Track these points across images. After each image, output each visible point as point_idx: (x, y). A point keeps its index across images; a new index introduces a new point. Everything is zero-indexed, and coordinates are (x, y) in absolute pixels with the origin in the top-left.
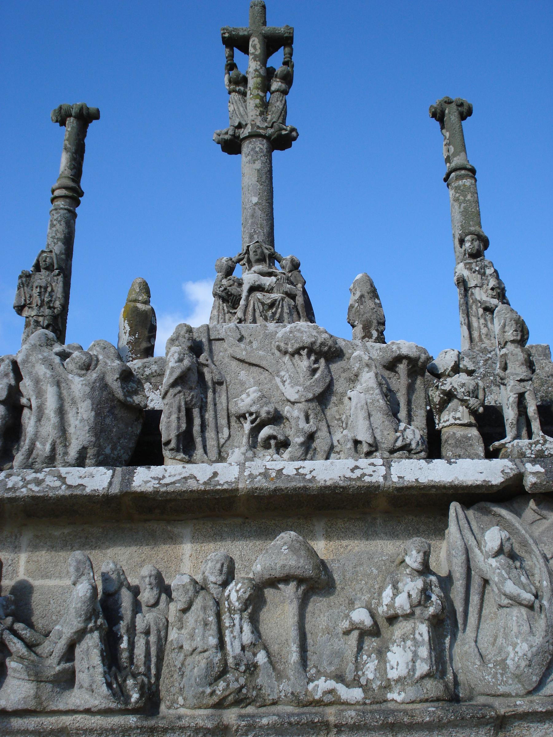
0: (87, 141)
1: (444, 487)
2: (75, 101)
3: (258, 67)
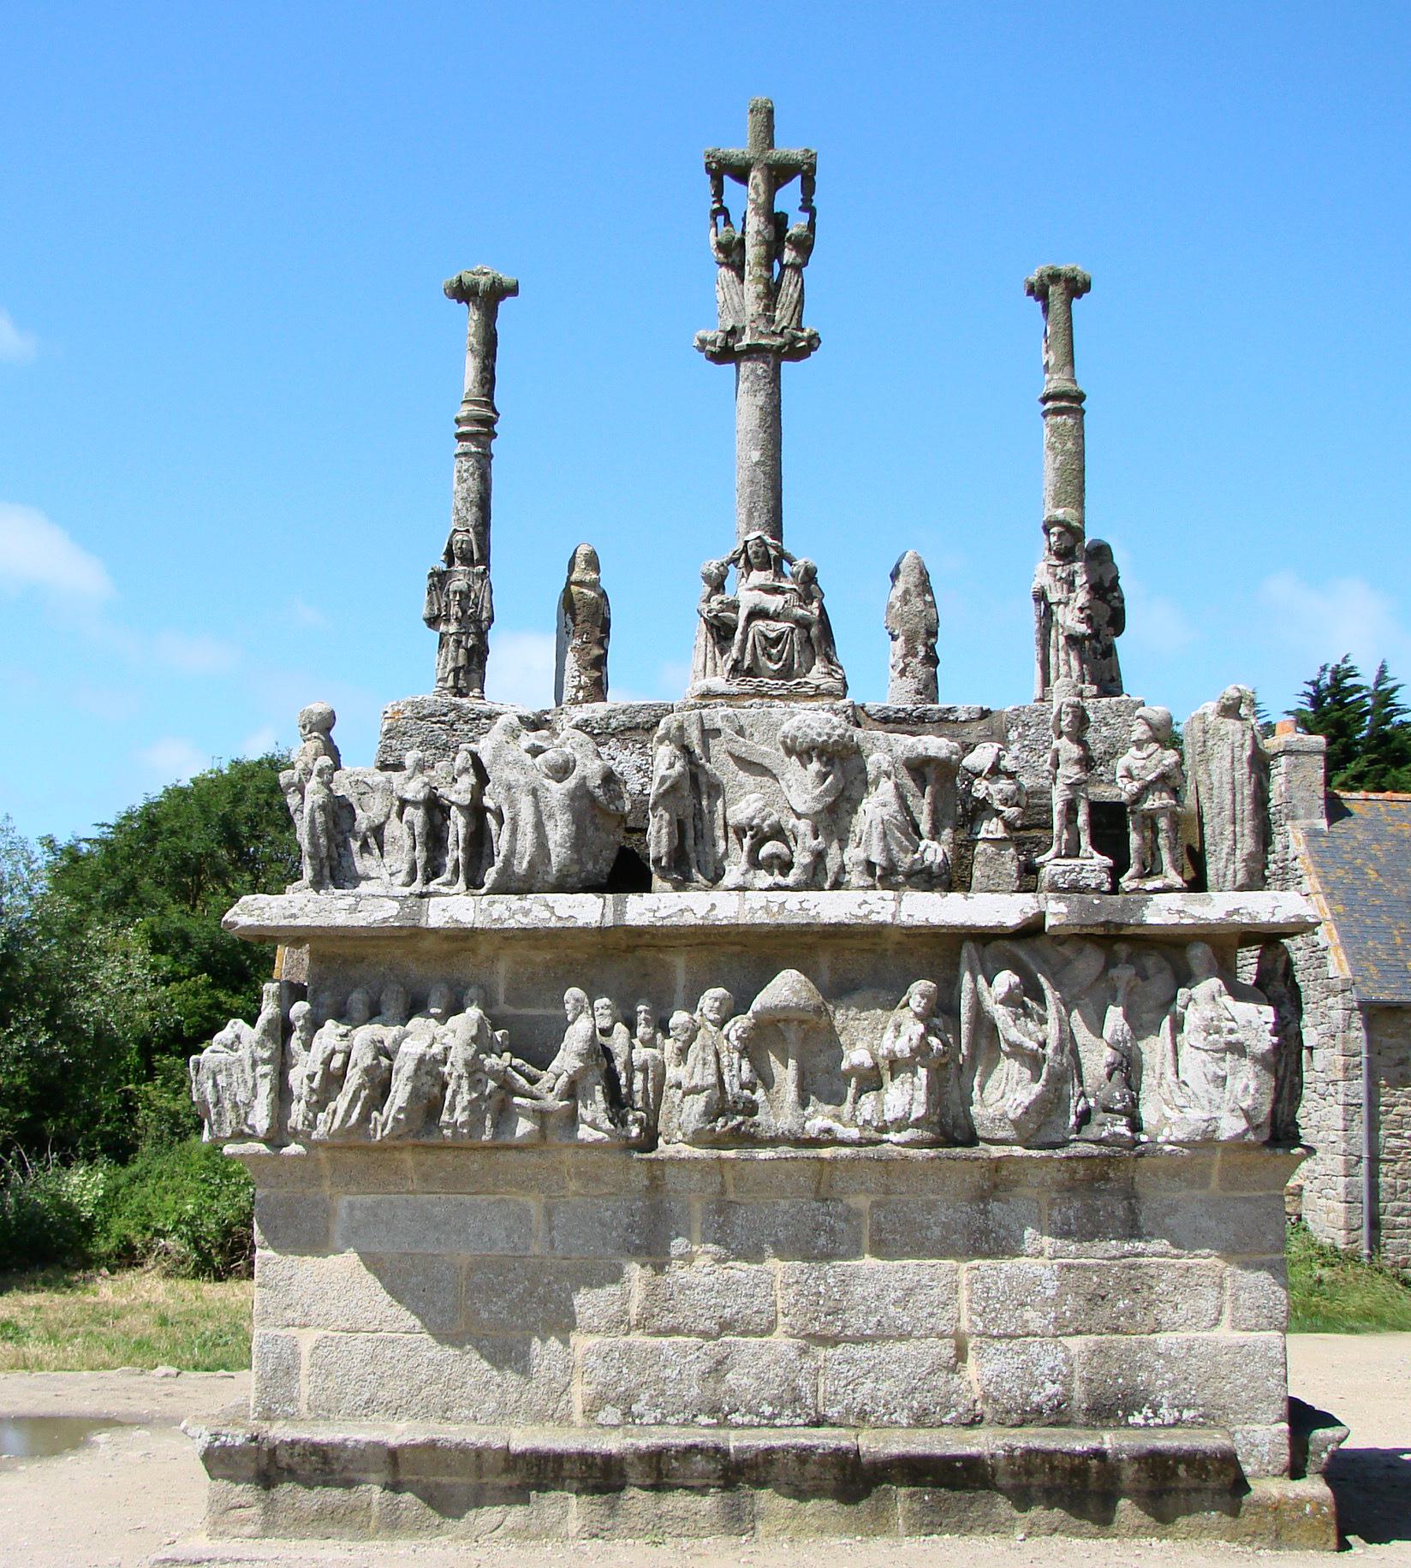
0: (500, 325)
1: (955, 927)
2: (482, 268)
3: (762, 227)
